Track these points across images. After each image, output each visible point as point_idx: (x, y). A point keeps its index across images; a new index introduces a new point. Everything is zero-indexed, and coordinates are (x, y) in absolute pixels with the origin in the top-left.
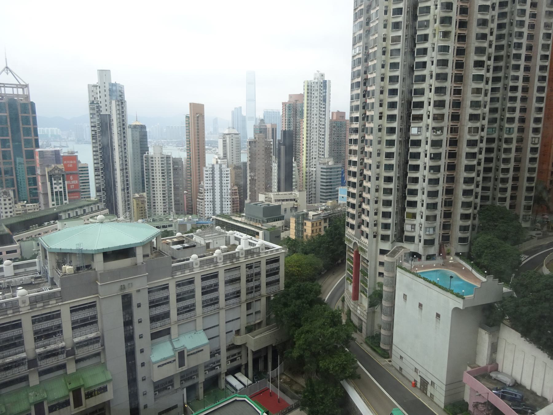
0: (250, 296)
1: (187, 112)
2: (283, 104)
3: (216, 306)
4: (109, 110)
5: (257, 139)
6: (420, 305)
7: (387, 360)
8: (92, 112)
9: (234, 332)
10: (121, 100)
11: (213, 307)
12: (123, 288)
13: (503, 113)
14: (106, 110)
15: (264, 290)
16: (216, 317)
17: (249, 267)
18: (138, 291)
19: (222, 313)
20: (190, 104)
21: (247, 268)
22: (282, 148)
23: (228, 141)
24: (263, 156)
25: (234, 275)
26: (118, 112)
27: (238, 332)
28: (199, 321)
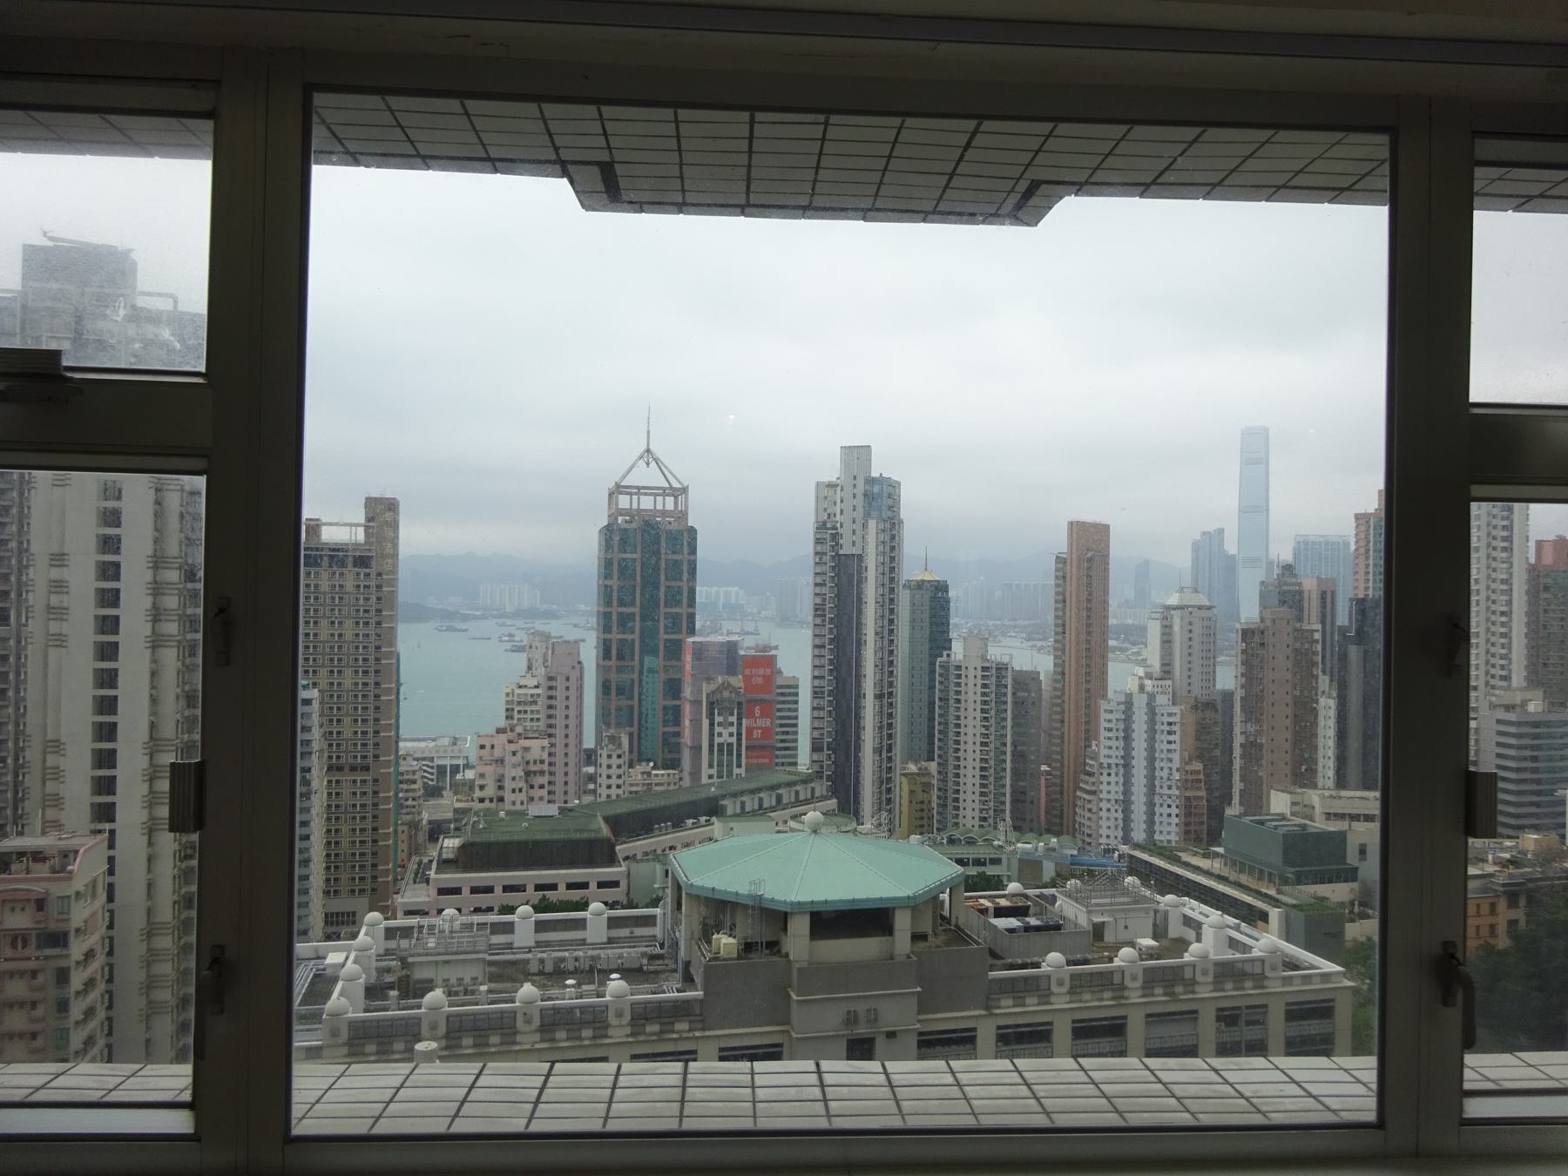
1: (1061, 543)
2: (1358, 517)
5: (1268, 623)
8: (819, 548)
12: (851, 1019)
18: (891, 1035)
20: (1071, 524)
21: (1219, 1019)
22: (1354, 652)
23: (1176, 628)
24: (1289, 676)
26: (881, 548)
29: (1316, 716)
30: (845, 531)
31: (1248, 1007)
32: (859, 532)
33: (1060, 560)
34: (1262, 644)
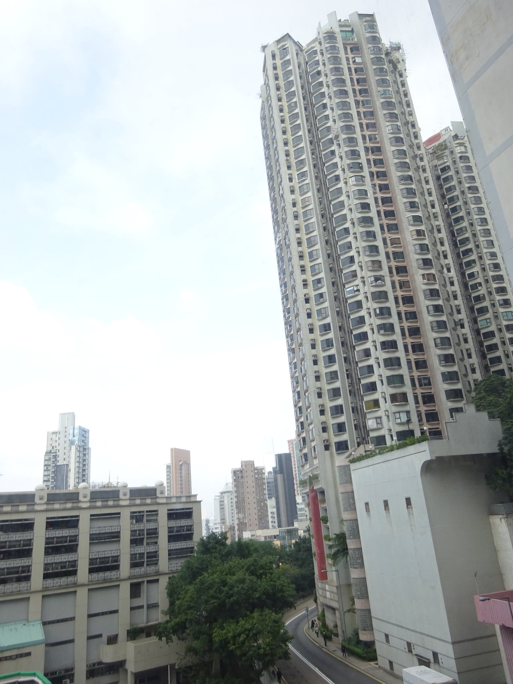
0: (137, 571)
1: (169, 461)
2: (289, 442)
3: (70, 579)
4: (67, 459)
5: (244, 467)
6: (386, 503)
7: (372, 663)
8: (46, 463)
9: (105, 638)
10: (84, 446)
11: (64, 581)
13: (491, 297)
14: (64, 459)
15: (164, 563)
16: (69, 599)
17: (137, 517)
19: (82, 593)
20: (172, 450)
21: (132, 517)
22: (279, 477)
23: (226, 502)
24: (254, 490)
25: (105, 527)
26: (78, 459)
27: (112, 640)
28: (36, 601)
29: (267, 507)
30: (60, 454)
31: (147, 512)
32: (67, 454)
33: (168, 467)
34: (242, 477)
